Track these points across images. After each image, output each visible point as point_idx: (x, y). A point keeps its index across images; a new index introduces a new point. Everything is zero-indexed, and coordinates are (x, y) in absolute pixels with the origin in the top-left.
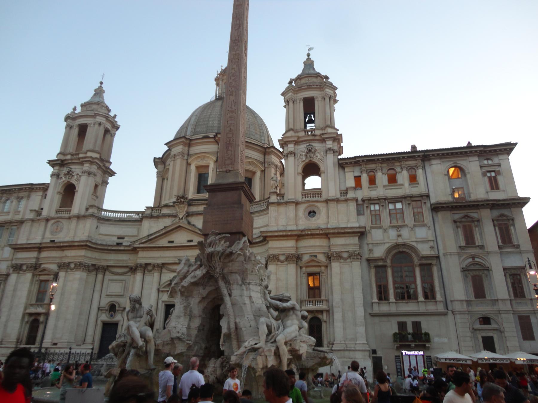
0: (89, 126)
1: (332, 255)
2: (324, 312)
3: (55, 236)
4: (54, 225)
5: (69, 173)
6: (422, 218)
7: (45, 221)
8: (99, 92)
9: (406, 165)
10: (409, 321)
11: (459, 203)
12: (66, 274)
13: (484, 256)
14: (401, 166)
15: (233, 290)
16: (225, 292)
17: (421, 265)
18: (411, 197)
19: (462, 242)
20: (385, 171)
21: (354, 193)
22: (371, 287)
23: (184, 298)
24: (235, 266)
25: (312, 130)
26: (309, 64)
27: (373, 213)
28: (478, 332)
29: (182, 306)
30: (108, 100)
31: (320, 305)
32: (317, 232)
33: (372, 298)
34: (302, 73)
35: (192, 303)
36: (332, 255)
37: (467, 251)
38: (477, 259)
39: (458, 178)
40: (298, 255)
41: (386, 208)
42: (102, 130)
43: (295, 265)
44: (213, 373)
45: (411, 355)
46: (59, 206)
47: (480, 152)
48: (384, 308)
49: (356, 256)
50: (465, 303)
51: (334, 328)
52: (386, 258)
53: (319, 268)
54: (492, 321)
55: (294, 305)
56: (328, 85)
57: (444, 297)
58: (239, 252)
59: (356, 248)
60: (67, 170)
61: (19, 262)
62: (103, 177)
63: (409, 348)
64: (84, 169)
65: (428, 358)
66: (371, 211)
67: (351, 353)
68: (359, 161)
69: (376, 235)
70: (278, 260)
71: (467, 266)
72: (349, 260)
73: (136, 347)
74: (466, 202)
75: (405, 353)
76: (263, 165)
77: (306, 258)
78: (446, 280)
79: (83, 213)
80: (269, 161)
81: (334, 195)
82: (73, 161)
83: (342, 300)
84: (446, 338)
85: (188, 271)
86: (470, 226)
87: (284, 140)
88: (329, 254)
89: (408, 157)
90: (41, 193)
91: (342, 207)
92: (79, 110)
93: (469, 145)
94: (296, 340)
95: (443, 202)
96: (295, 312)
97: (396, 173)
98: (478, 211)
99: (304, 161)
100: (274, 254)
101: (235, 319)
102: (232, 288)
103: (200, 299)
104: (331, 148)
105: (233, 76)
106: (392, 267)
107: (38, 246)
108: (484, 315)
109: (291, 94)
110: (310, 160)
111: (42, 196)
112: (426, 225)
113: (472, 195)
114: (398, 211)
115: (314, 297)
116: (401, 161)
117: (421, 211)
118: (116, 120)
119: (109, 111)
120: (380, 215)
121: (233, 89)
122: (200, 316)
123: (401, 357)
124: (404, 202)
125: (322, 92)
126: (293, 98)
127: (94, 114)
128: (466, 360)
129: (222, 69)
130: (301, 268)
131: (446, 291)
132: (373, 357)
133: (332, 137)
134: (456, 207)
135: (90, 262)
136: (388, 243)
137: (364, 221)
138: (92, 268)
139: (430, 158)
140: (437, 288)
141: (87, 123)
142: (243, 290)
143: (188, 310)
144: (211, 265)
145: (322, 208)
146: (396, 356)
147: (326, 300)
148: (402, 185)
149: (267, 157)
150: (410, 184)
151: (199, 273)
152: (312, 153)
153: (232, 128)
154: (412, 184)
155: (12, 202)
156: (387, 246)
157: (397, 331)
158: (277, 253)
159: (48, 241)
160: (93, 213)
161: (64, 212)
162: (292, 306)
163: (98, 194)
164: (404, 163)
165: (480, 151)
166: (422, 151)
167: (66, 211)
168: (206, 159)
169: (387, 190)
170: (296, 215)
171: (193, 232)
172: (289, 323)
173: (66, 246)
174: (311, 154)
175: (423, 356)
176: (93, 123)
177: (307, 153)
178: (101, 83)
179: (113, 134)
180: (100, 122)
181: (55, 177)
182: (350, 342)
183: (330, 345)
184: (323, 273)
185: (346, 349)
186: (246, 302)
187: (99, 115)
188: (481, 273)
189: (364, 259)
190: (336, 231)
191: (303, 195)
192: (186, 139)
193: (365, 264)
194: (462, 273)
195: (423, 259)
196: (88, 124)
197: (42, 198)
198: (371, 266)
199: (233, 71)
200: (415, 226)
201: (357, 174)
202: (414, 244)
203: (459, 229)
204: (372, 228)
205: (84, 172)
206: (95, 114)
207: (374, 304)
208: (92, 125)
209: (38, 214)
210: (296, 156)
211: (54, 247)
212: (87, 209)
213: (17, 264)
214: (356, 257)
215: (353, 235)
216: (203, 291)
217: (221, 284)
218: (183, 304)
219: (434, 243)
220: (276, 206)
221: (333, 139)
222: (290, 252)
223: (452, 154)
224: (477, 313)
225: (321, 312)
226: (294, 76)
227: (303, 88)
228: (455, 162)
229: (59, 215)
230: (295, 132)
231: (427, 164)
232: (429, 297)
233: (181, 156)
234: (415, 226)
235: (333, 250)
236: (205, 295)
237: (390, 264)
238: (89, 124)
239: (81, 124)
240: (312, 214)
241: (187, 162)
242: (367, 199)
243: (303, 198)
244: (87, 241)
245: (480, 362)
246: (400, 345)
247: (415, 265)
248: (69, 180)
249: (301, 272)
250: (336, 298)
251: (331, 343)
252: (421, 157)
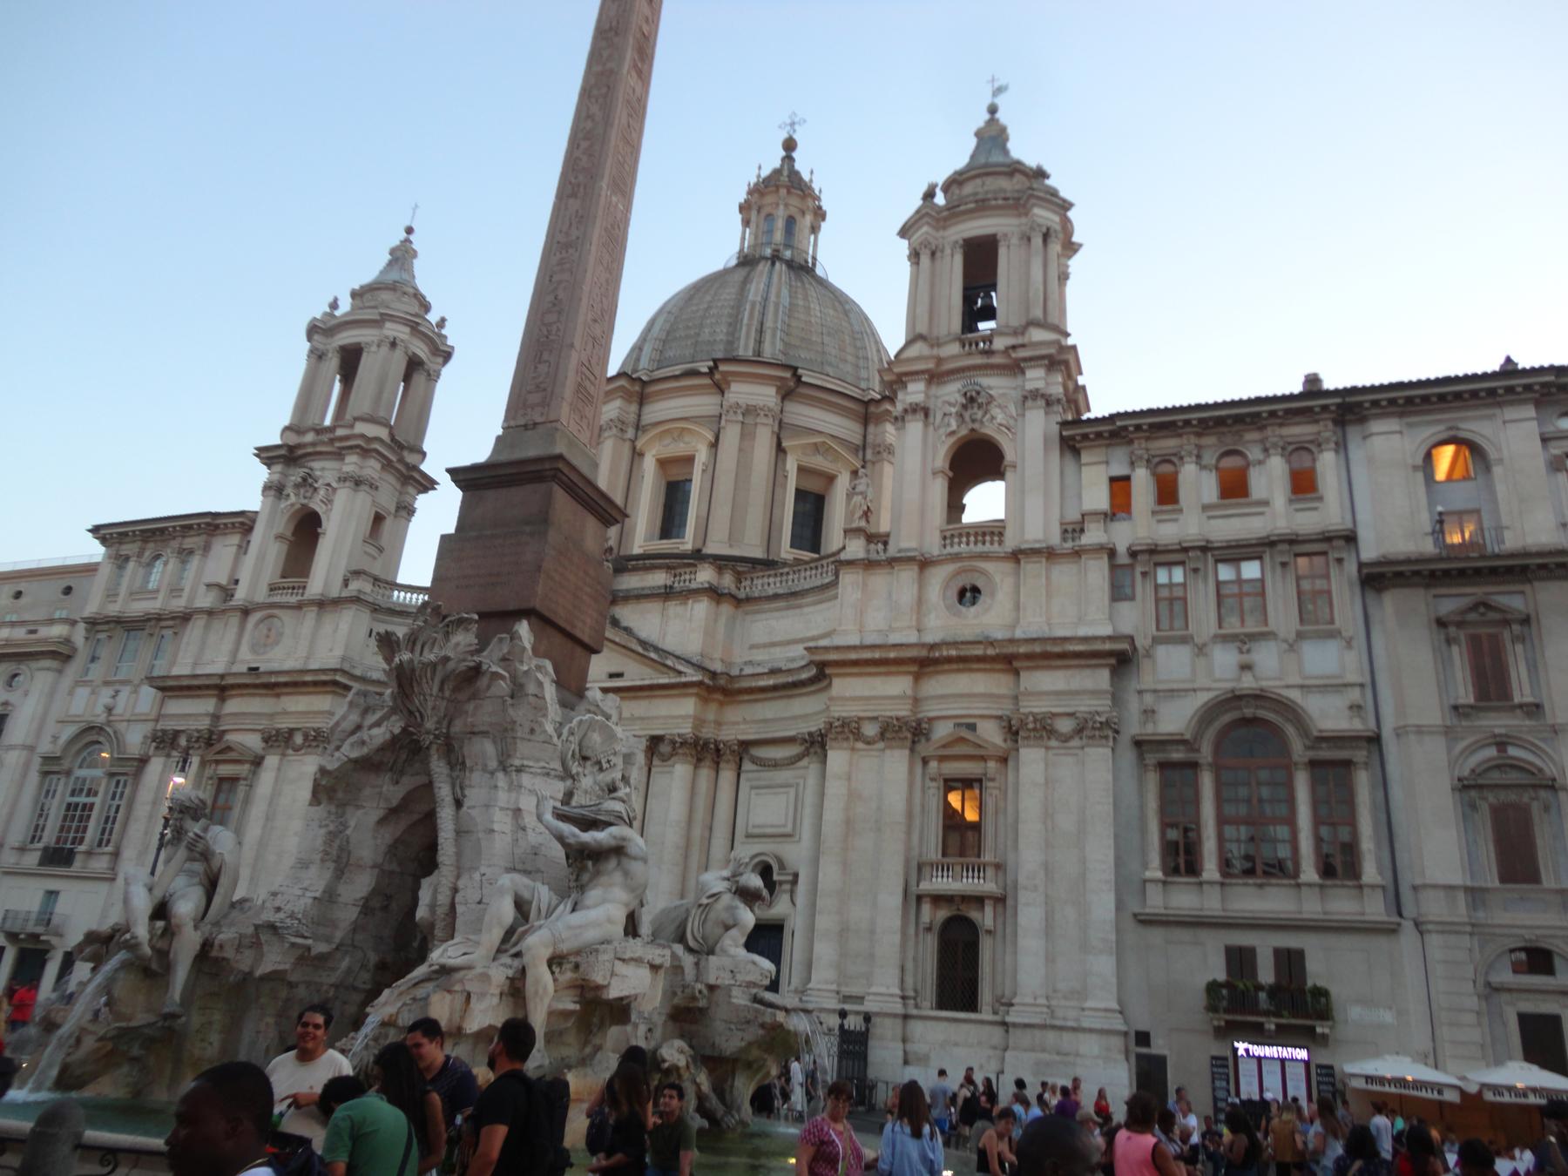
1: (1023, 723)
2: (987, 902)
4: (261, 626)
5: (307, 482)
6: (1327, 610)
8: (402, 255)
9: (1281, 437)
10: (1265, 946)
11: (1457, 559)
12: (281, 760)
13: (1544, 740)
14: (1262, 441)
15: (470, 786)
16: (444, 792)
17: (1313, 764)
18: (1293, 541)
19: (1462, 691)
20: (1210, 458)
21: (1106, 531)
22: (1143, 831)
23: (333, 809)
24: (483, 713)
25: (989, 339)
26: (992, 136)
27: (1164, 593)
28: (1505, 997)
29: (323, 831)
30: (426, 278)
31: (976, 880)
32: (978, 651)
33: (1145, 866)
34: (968, 165)
35: (352, 823)
36: (1023, 723)
37: (1477, 723)
38: (1512, 751)
39: (1466, 478)
40: (919, 722)
41: (1205, 579)
42: (399, 363)
43: (906, 752)
44: (371, 1043)
45: (1265, 1057)
46: (279, 572)
47: (1545, 391)
48: (1184, 899)
49: (1099, 729)
50: (1461, 896)
51: (1015, 953)
52: (1195, 739)
53: (982, 764)
54: (1557, 962)
55: (624, 839)
56: (1041, 194)
57: (1389, 874)
58: (494, 669)
59: (1103, 705)
61: (170, 725)
62: (401, 493)
63: (1258, 1035)
65: (1324, 1071)
66: (1157, 587)
67: (1066, 1036)
68: (1125, 428)
69: (1171, 664)
70: (858, 735)
71: (1478, 771)
72: (1075, 742)
73: (132, 946)
74: (1483, 557)
75: (1247, 1051)
76: (861, 454)
77: (942, 731)
78: (1398, 816)
79: (335, 592)
80: (877, 442)
81: (1040, 536)
83: (1047, 868)
84: (1390, 1008)
85: (359, 728)
86: (1495, 641)
87: (897, 370)
88: (1013, 722)
89: (1288, 412)
90: (235, 539)
91: (1064, 573)
92: (345, 306)
93: (1510, 367)
94: (597, 951)
95: (1402, 557)
96: (625, 860)
97: (1248, 465)
98: (1527, 588)
99: (953, 433)
100: (844, 718)
101: (458, 877)
102: (467, 783)
103: (380, 813)
104: (1037, 390)
105: (586, 138)
106: (1217, 768)
107: (216, 681)
108: (1531, 941)
109: (925, 229)
110: (973, 430)
111: (240, 546)
112: (1340, 633)
113: (1507, 535)
114: (1247, 588)
115: (962, 854)
116: (1262, 428)
117: (1326, 587)
118: (444, 332)
119: (426, 307)
120: (1184, 600)
121: (581, 178)
122: (374, 867)
123: (1231, 1062)
124: (1267, 558)
125: (1024, 220)
126: (931, 240)
127: (378, 318)
128: (1439, 1088)
129: (759, 176)
130: (925, 761)
131: (1398, 855)
132: (1139, 1057)
133: (1042, 357)
134: (1447, 573)
136: (1209, 690)
137: (1134, 619)
139: (1366, 413)
140: (1367, 844)
141: (359, 344)
142: (496, 787)
143: (338, 842)
144: (413, 708)
145: (999, 576)
146: (1213, 1058)
147: (998, 867)
148: (1266, 503)
149: (871, 429)
151: (379, 735)
152: (980, 406)
153: (561, 295)
154: (1299, 500)
155: (166, 564)
156: (1203, 698)
157: (1221, 976)
158: (854, 714)
159: (244, 669)
160: (359, 591)
162: (613, 843)
164: (1274, 433)
165: (1543, 385)
166: (1336, 393)
167: (294, 588)
168: (687, 439)
169: (1213, 522)
170: (920, 601)
171: (623, 651)
172: (593, 894)
173: (286, 684)
174: (975, 410)
175: (1307, 1063)
177: (964, 407)
178: (409, 230)
182: (1063, 1003)
183: (1002, 1008)
184: (993, 780)
185: (1048, 1022)
186: (496, 827)
187: (392, 318)
188: (1526, 799)
189: (1125, 739)
190: (1038, 648)
191: (945, 538)
192: (632, 380)
193: (1128, 756)
194: (1457, 794)
195: (1324, 745)
198: (1147, 762)
199: (589, 125)
200: (1300, 636)
201: (1119, 470)
202: (1295, 695)
203: (1455, 649)
204: (1156, 641)
205: (341, 480)
206: (382, 314)
207: (1148, 885)
208: (374, 348)
210: (931, 419)
211: (256, 686)
212: (346, 583)
213: (164, 732)
214: (1097, 733)
215: (1094, 662)
216: (390, 790)
217: (438, 767)
218: (327, 826)
219: (1363, 695)
220: (861, 571)
221: (1046, 362)
222: (893, 714)
223: (1442, 398)
224: (1506, 931)
225: (979, 900)
226: (940, 178)
227: (962, 208)
228: (1450, 424)
229: (277, 599)
230: (932, 346)
231: (1353, 433)
232: (1339, 869)
233: (614, 431)
234: (1300, 636)
235: (1026, 710)
236: (394, 803)
237: (1210, 759)
239: (351, 345)
240: (968, 595)
241: (634, 448)
242: (1144, 548)
243: (945, 546)
244: (335, 671)
245: (1489, 1096)
246: (1227, 1022)
247: (1296, 764)
249: (924, 774)
250: (1029, 859)
251: (1004, 1001)
252: (1332, 412)
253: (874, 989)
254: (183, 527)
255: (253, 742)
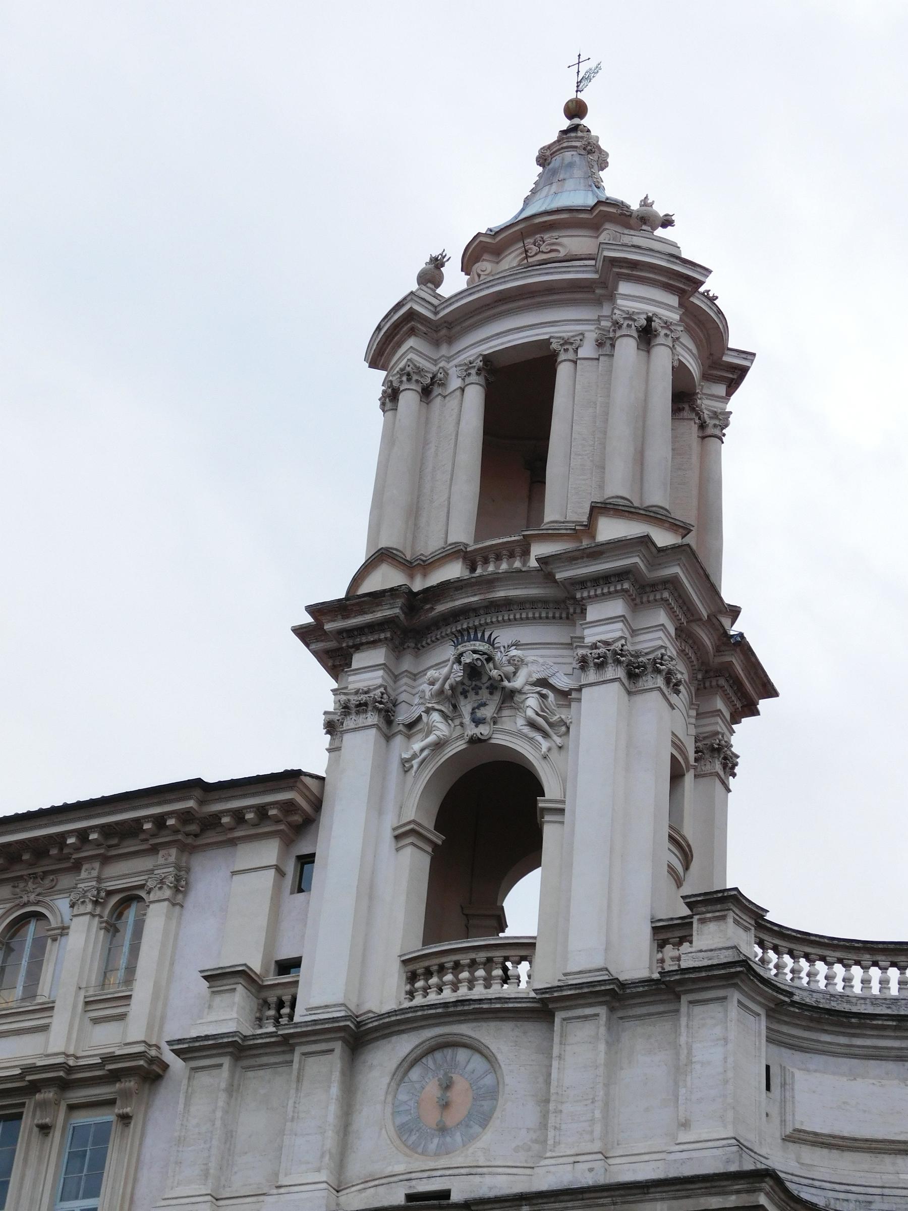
0: (562, 356)
3: (443, 1162)
4: (415, 1074)
7: (338, 1046)
60: (467, 659)
82: (501, 594)
111: (280, 872)
141: (547, 342)
161: (481, 973)
163: (690, 832)
176: (591, 336)
178: (576, 110)
179: (715, 415)
180: (649, 320)
181: (372, 718)
196: (554, 346)
197: (277, 889)
208: (587, 350)
209: (265, 1004)
238: (566, 342)
248: (484, 730)
254: (107, 831)
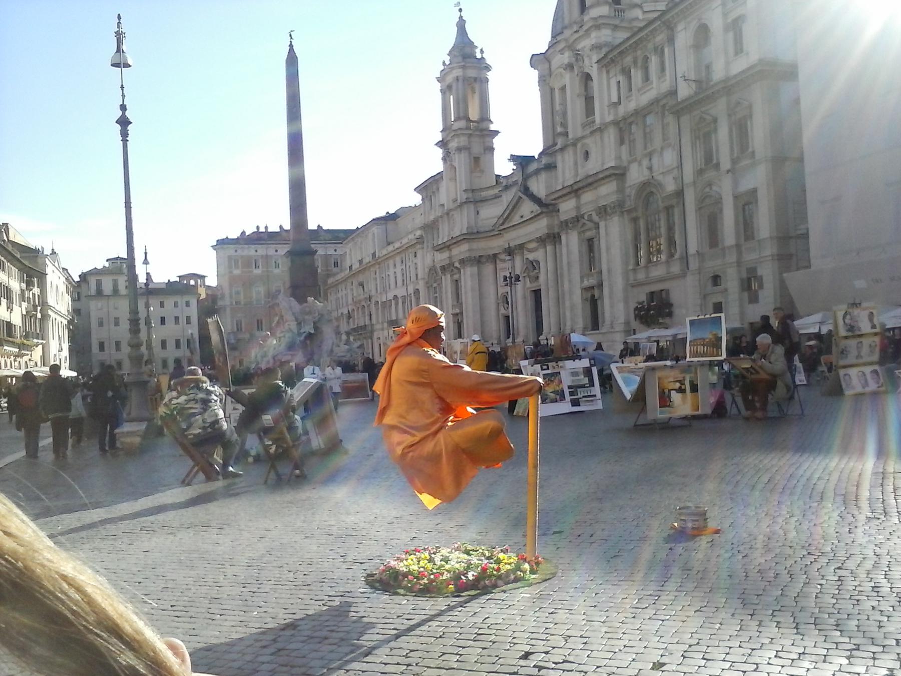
8: (461, 25)
64: (456, 145)
82: (448, 139)
83: (609, 271)
99: (577, 75)
118: (484, 56)
135: (477, 254)
138: (483, 260)
150: (659, 78)
170: (576, 163)
178: (460, 10)
184: (596, 237)
200: (662, 149)
204: (630, 162)
219: (678, 170)
225: (592, 288)
253: (578, 327)
255: (457, 265)
